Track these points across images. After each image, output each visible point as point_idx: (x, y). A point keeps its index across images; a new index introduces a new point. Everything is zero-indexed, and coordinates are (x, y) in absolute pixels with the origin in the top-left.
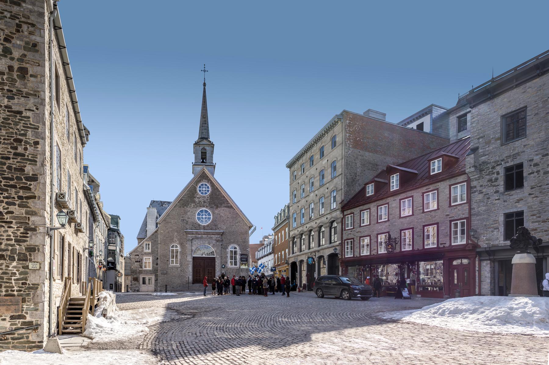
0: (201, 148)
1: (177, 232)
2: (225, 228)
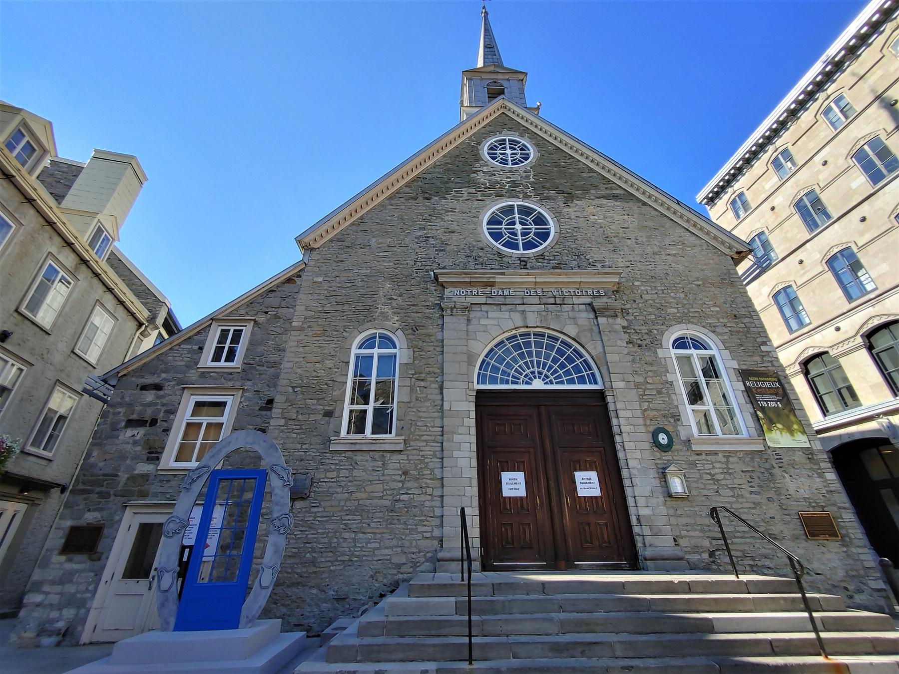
1: (391, 279)
2: (621, 262)
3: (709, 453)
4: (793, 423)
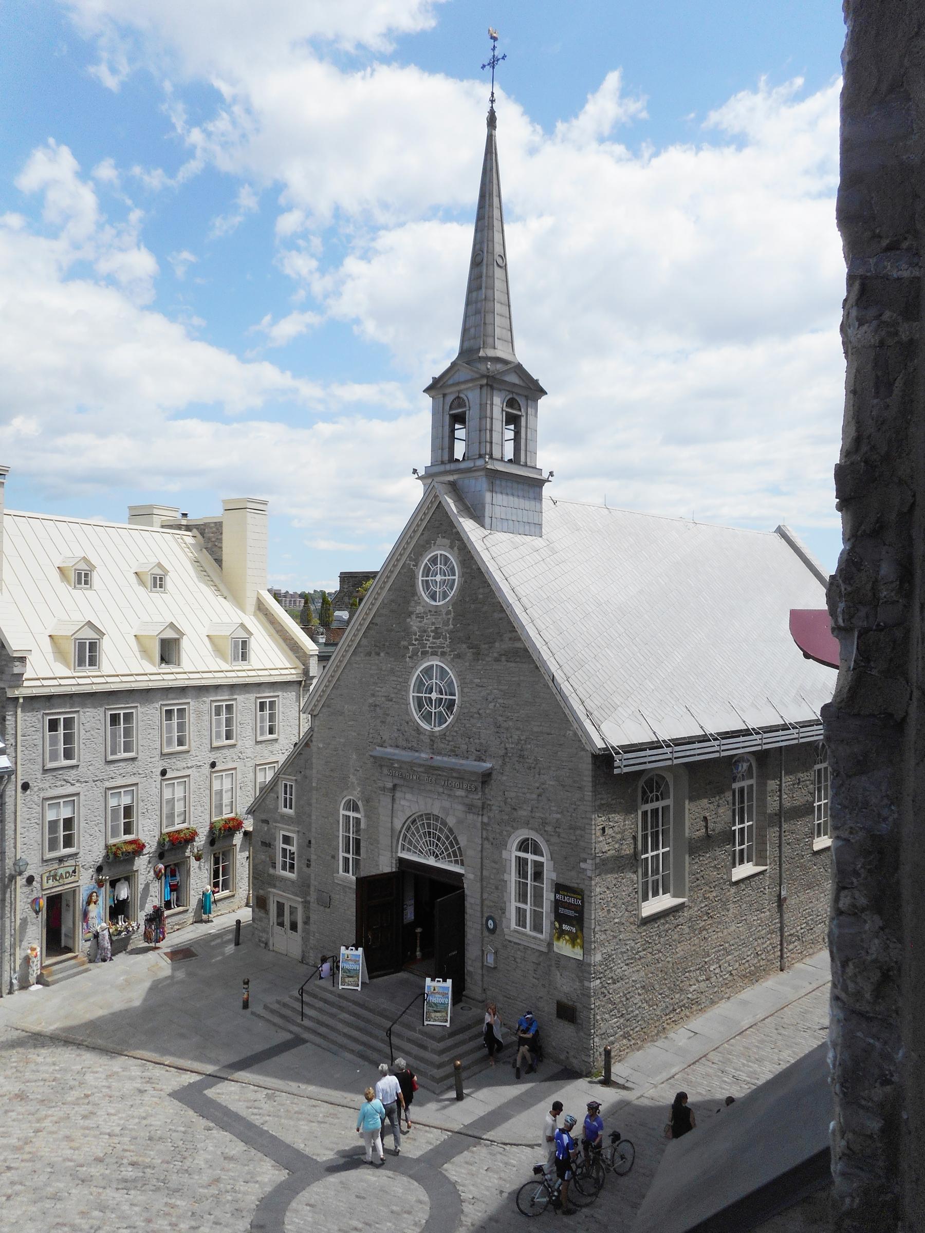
0: (450, 399)
3: (515, 943)
4: (577, 937)
